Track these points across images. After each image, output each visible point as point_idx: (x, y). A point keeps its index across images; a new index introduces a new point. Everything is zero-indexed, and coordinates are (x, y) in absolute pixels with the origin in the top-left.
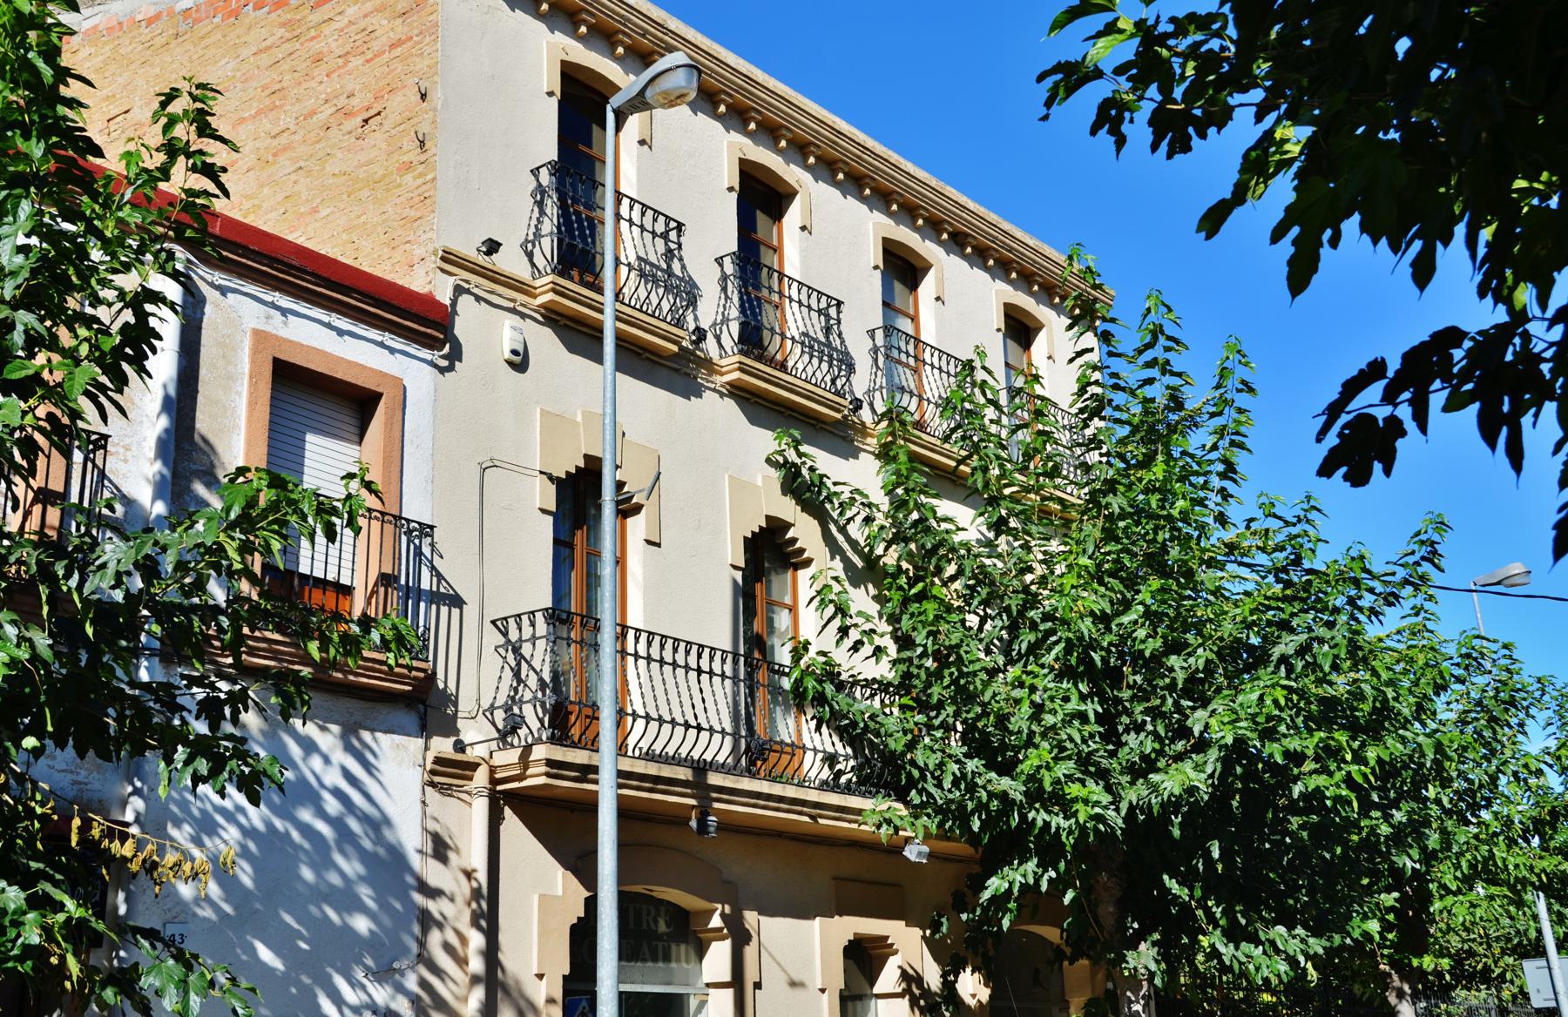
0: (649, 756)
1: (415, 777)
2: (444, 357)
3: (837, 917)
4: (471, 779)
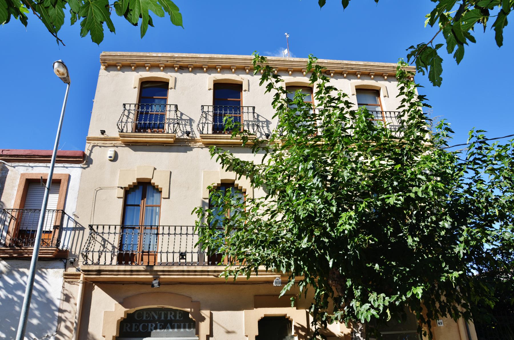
0: (167, 264)
1: (61, 280)
2: (85, 164)
3: (255, 309)
4: (79, 279)
